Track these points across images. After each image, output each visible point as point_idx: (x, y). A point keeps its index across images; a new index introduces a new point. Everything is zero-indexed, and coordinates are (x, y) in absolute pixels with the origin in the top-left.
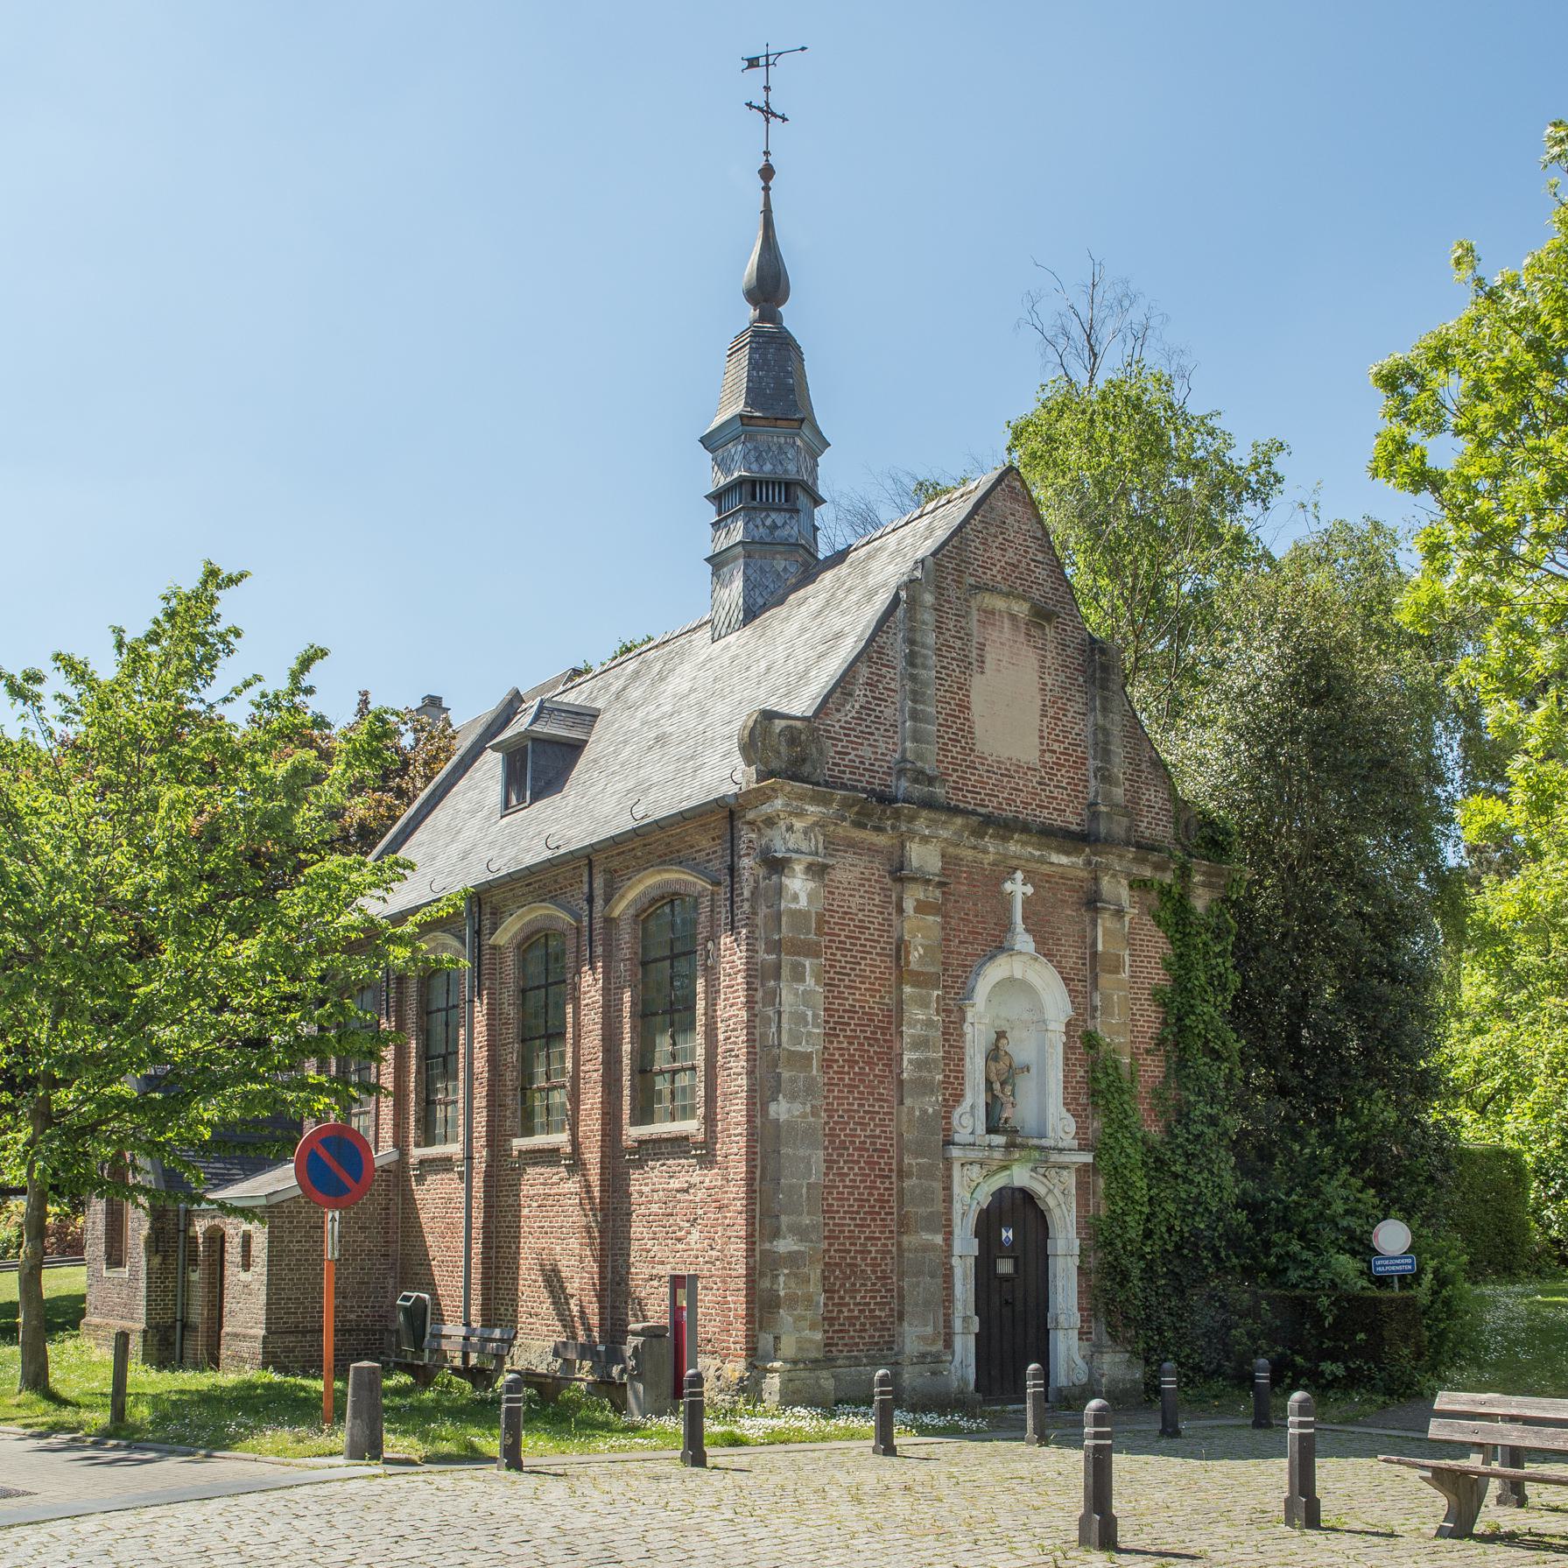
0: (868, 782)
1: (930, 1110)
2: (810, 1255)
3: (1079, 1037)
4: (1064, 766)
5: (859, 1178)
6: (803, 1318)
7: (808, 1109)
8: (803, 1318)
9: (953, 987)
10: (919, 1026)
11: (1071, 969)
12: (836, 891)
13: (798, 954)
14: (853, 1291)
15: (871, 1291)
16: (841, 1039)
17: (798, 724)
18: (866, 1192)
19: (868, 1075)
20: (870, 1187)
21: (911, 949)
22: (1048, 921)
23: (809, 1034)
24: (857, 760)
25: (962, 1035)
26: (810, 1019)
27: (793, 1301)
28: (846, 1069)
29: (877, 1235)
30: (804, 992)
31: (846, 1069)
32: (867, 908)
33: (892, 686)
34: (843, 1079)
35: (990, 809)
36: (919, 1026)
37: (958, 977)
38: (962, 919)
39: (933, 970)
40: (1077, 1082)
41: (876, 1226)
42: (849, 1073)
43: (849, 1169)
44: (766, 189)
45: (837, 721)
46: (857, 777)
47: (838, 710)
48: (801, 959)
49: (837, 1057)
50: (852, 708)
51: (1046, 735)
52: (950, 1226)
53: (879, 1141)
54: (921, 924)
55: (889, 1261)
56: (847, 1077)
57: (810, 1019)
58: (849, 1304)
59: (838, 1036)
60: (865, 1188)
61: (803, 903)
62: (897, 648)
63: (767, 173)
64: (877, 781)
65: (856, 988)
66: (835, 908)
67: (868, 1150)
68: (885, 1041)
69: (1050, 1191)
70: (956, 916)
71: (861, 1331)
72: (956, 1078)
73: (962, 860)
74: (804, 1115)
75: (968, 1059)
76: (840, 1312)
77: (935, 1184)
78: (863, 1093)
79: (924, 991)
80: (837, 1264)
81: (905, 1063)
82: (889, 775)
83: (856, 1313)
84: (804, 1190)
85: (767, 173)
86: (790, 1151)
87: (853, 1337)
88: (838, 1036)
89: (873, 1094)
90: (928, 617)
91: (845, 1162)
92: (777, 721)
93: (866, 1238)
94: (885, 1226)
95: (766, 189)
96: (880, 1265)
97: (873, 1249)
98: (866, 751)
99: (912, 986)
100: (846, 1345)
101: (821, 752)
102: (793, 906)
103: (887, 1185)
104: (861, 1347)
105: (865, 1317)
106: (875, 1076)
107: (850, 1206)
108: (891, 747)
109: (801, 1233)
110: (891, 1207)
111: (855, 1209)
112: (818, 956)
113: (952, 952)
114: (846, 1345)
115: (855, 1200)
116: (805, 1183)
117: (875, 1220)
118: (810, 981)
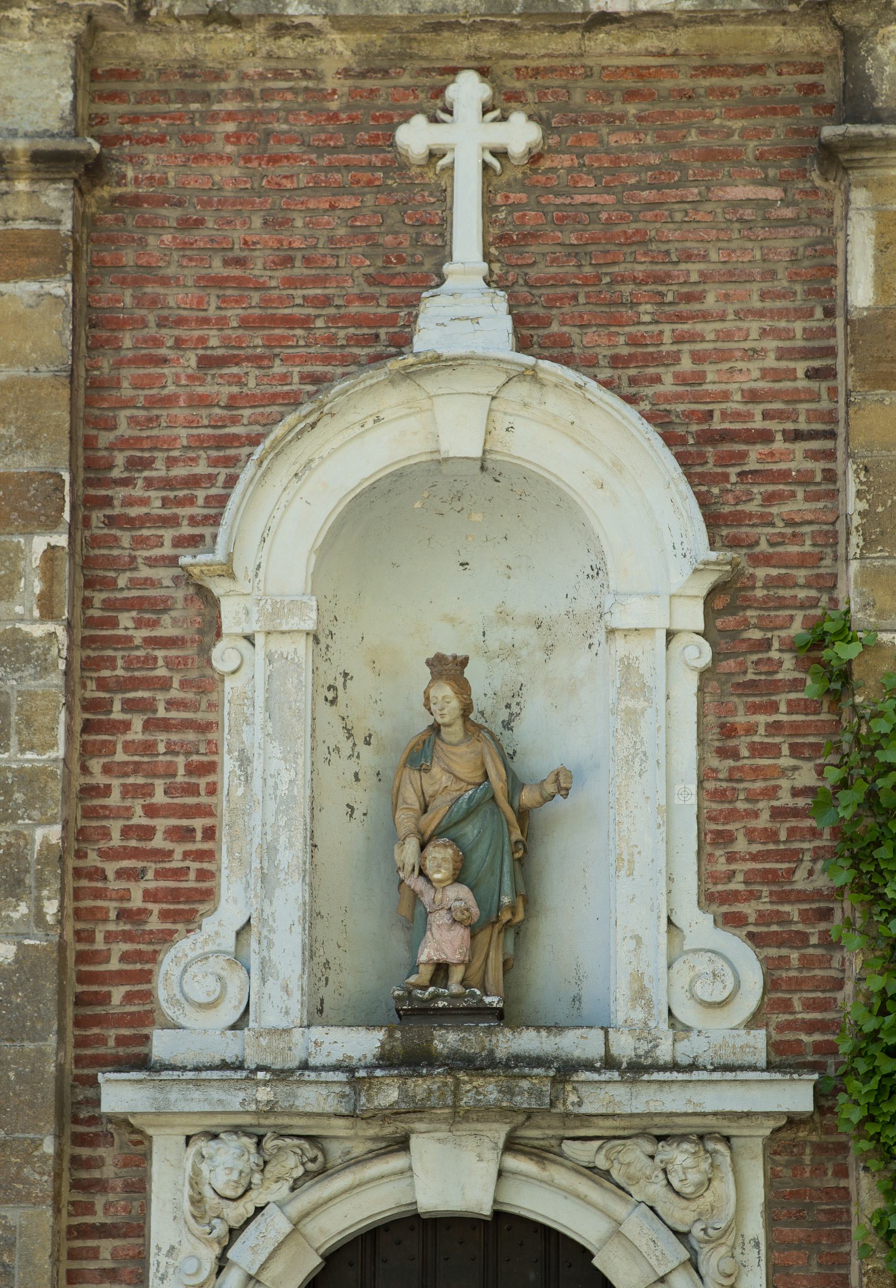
3: (789, 646)
9: (172, 521)
11: (753, 397)
22: (642, 240)
37: (194, 481)
38: (219, 282)
40: (778, 813)
69: (617, 1232)
70: (190, 274)
72: (186, 834)
73: (218, 76)
75: (229, 764)
113: (169, 401)
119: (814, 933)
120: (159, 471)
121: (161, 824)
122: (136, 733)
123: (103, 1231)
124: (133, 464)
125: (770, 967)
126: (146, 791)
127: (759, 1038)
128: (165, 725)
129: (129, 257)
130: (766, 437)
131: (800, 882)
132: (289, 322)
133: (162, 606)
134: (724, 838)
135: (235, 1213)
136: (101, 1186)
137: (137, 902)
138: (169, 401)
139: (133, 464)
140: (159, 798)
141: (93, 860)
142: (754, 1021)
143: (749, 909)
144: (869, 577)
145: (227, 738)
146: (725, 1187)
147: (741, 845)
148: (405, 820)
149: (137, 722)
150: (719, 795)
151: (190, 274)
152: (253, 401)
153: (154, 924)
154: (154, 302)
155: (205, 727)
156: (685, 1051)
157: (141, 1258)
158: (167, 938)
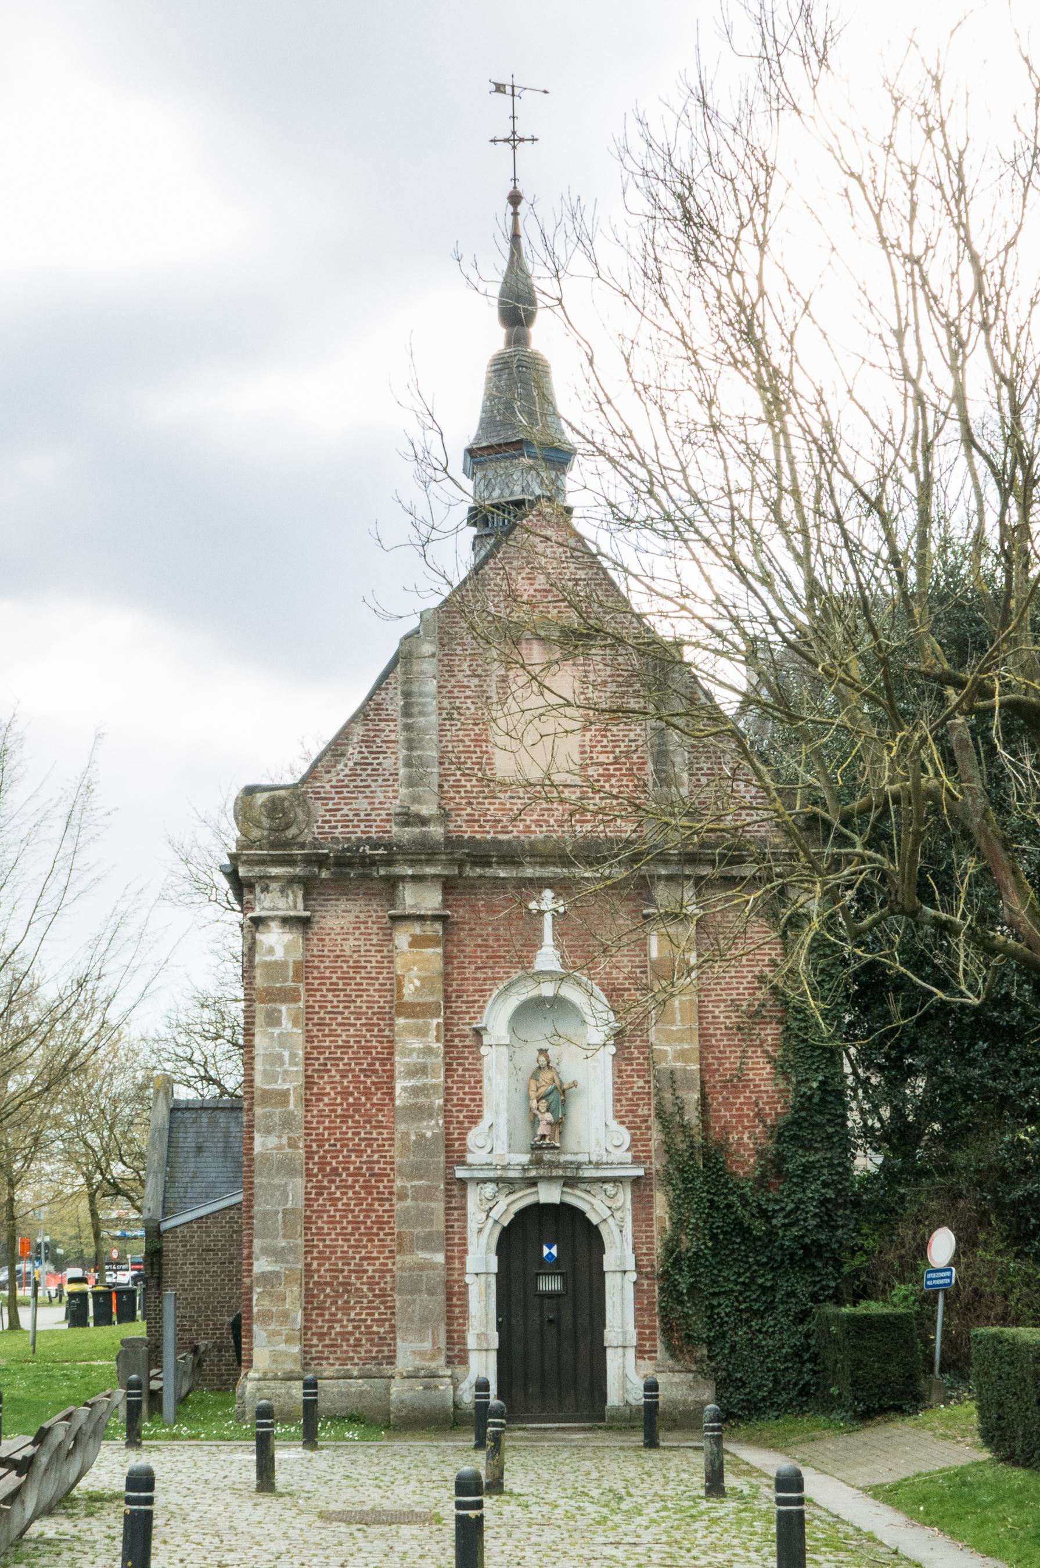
0: (363, 832)
1: (429, 1134)
2: (286, 1276)
4: (613, 776)
5: (353, 1202)
6: (278, 1333)
7: (284, 1141)
8: (278, 1333)
10: (415, 1055)
12: (327, 938)
13: (274, 1001)
14: (346, 1309)
15: (367, 1308)
16: (333, 1073)
17: (283, 793)
18: (362, 1215)
19: (364, 1105)
20: (366, 1210)
21: (406, 982)
23: (286, 1072)
24: (351, 813)
25: (480, 1058)
26: (287, 1059)
27: (267, 1317)
28: (339, 1101)
29: (375, 1254)
30: (279, 1036)
31: (339, 1101)
32: (363, 948)
33: (393, 737)
34: (335, 1111)
35: (515, 834)
36: (415, 1055)
37: (475, 1001)
38: (480, 946)
39: (431, 999)
40: (634, 1094)
41: (373, 1247)
42: (341, 1104)
43: (343, 1193)
44: (515, 214)
45: (326, 784)
46: (350, 829)
47: (328, 772)
48: (278, 1006)
49: (328, 1090)
50: (343, 769)
51: (588, 749)
52: (465, 1244)
53: (377, 1166)
54: (417, 957)
55: (389, 1279)
56: (339, 1108)
57: (287, 1059)
58: (341, 1321)
59: (329, 1071)
60: (360, 1211)
61: (279, 955)
62: (395, 704)
63: (515, 199)
64: (374, 829)
65: (350, 1025)
66: (326, 953)
67: (364, 1175)
68: (384, 1071)
70: (472, 944)
71: (355, 1346)
72: (473, 1100)
74: (280, 1148)
76: (331, 1327)
77: (433, 1205)
78: (358, 1122)
79: (421, 1021)
80: (326, 1284)
81: (398, 1091)
82: (388, 821)
83: (350, 1329)
84: (280, 1216)
85: (515, 199)
86: (264, 1181)
87: (346, 1352)
88: (329, 1071)
89: (370, 1122)
90: (429, 667)
91: (337, 1188)
92: (258, 795)
93: (362, 1259)
94: (384, 1246)
95: (515, 214)
96: (378, 1283)
97: (370, 1268)
98: (362, 804)
99: (407, 1017)
100: (337, 1359)
101: (309, 814)
102: (268, 959)
103: (387, 1207)
104: (356, 1361)
105: (361, 1333)
106: (373, 1105)
107: (343, 1228)
108: (391, 795)
109: (277, 1254)
110: (392, 1228)
111: (349, 1230)
112: (296, 999)
113: (467, 979)
114: (337, 1359)
115: (348, 1223)
116: (280, 1209)
117: (371, 1241)
118: (286, 1024)
119: (643, 1126)
120: (465, 998)
121: (468, 1097)
122: (460, 1072)
123: (455, 1209)
124: (458, 997)
125: (633, 1135)
126: (463, 1088)
127: (629, 1155)
128: (468, 1070)
129: (456, 938)
130: (629, 990)
131: (640, 1112)
132: (500, 957)
133: (467, 1036)
134: (619, 1101)
135: (491, 1204)
136: (454, 1196)
137: (461, 1119)
138: (467, 979)
139: (458, 997)
140: (467, 1090)
141: (449, 1107)
142: (628, 1150)
143: (626, 1120)
144: (657, 1031)
145: (485, 1073)
146: (621, 1196)
147: (624, 1102)
148: (533, 1094)
149: (460, 1068)
150: (618, 1089)
151: (472, 944)
152: (490, 979)
153: (466, 1125)
154: (462, 951)
155: (479, 1070)
156: (611, 1158)
157: (465, 1215)
158: (469, 1128)
